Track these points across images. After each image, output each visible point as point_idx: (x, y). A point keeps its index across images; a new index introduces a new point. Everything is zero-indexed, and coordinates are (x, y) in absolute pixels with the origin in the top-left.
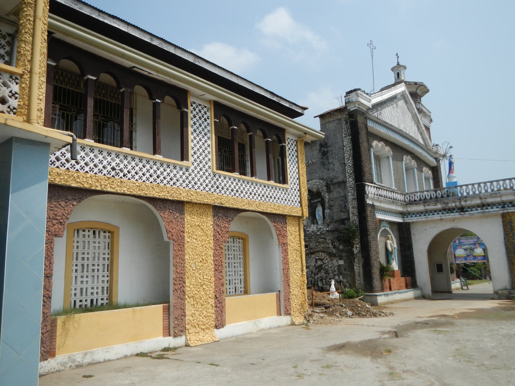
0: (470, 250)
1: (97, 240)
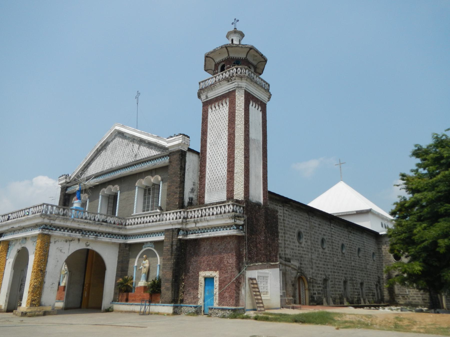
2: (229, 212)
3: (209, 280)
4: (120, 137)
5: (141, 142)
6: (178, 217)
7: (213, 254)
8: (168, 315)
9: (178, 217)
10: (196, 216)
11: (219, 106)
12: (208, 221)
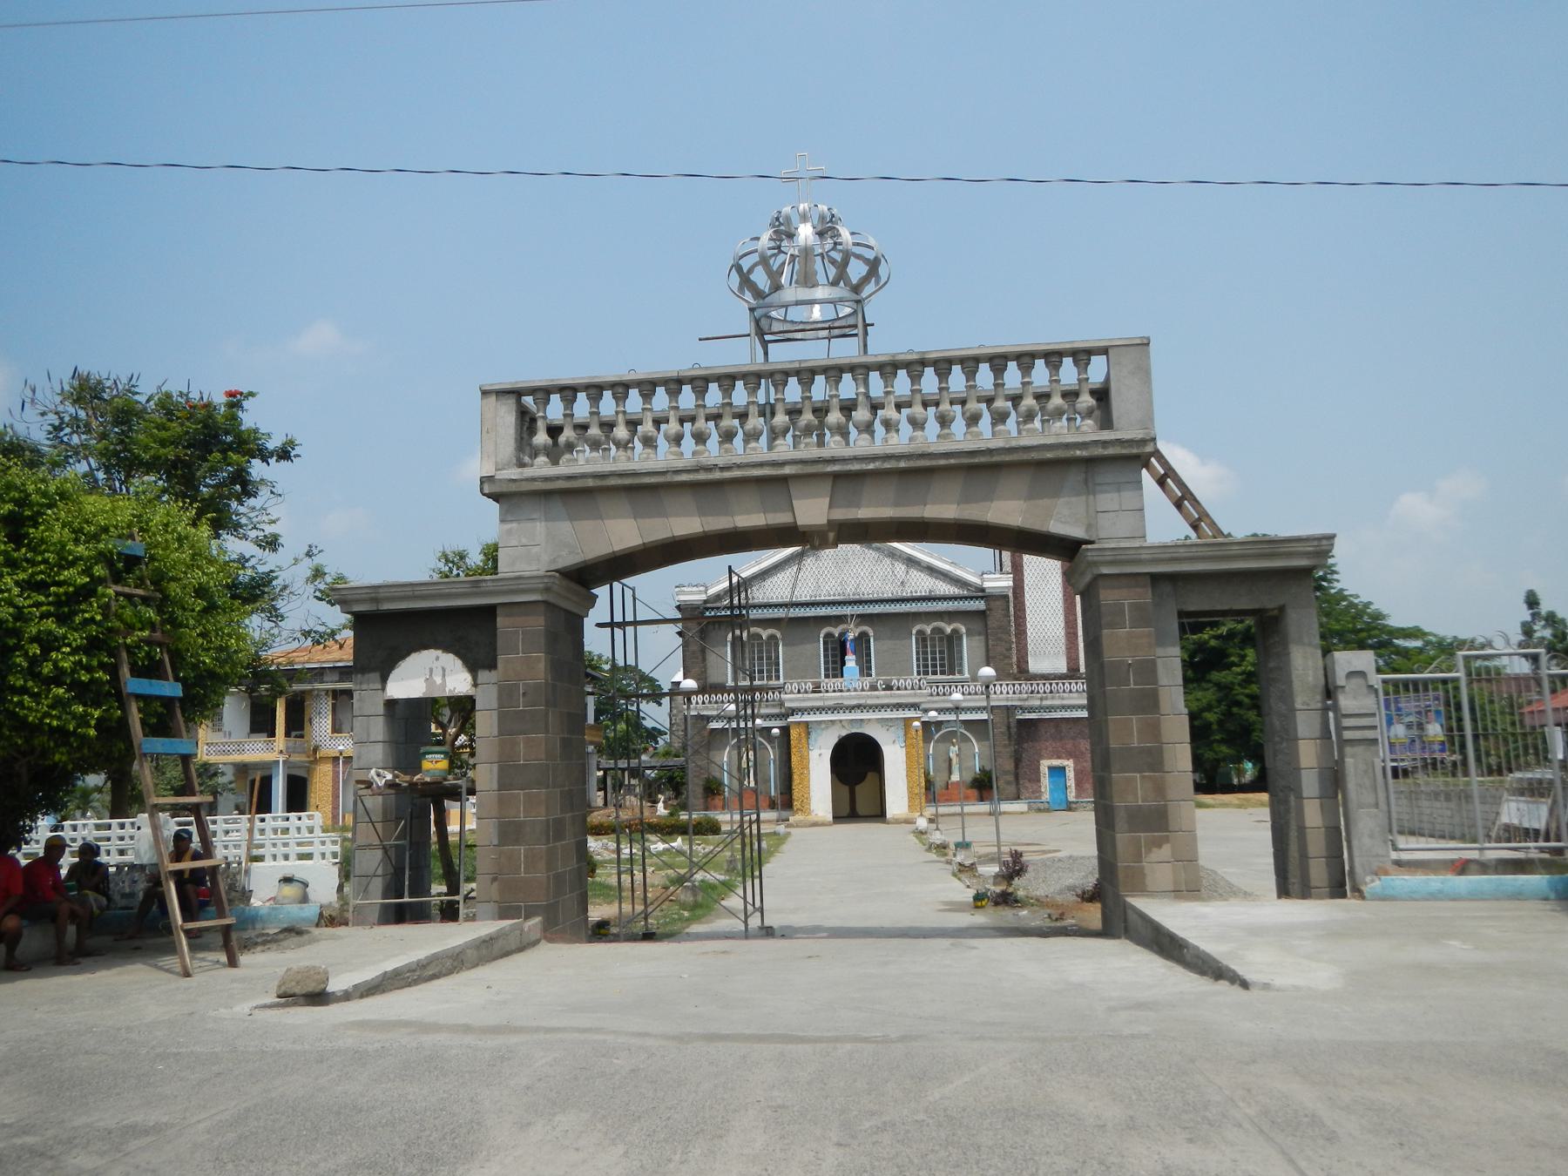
3: (1058, 771)
6: (1017, 692)
7: (1061, 739)
8: (1022, 813)
10: (1041, 691)
12: (1063, 699)
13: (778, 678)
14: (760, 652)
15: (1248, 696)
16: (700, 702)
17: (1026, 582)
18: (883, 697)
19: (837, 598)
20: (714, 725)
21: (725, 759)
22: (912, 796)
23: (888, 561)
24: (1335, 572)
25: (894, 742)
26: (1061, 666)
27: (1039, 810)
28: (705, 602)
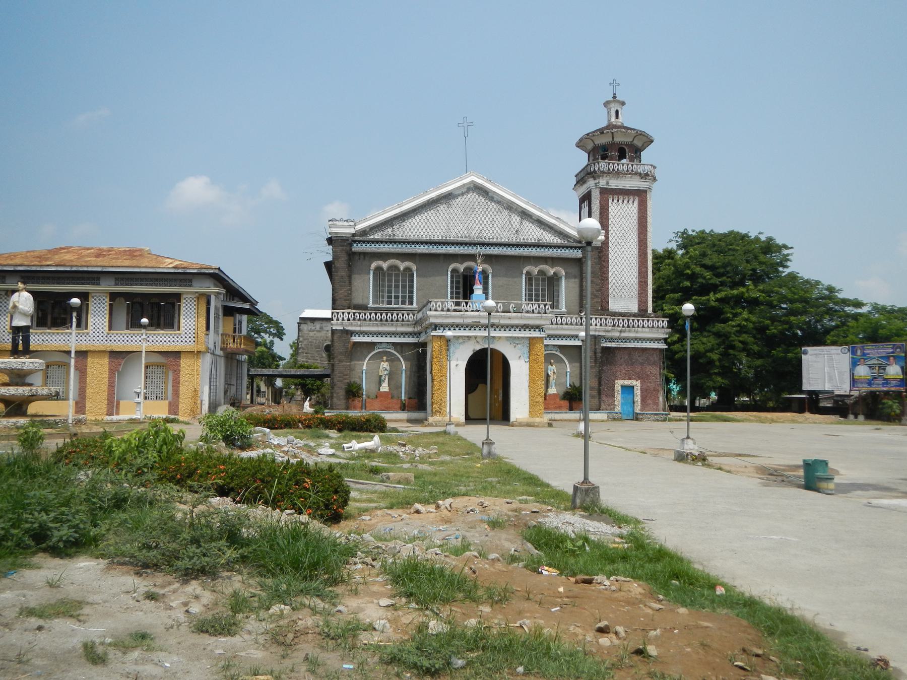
0: (879, 367)
1: (60, 369)
2: (663, 327)
4: (479, 194)
5: (525, 215)
6: (603, 324)
7: (632, 364)
8: (603, 421)
9: (603, 324)
11: (623, 201)
12: (637, 332)
13: (412, 303)
14: (397, 281)
15: (740, 342)
16: (346, 319)
17: (610, 239)
18: (514, 319)
19: (464, 239)
20: (356, 339)
21: (364, 368)
22: (533, 404)
23: (506, 212)
24: (788, 260)
25: (520, 357)
26: (634, 307)
27: (614, 419)
28: (354, 235)
